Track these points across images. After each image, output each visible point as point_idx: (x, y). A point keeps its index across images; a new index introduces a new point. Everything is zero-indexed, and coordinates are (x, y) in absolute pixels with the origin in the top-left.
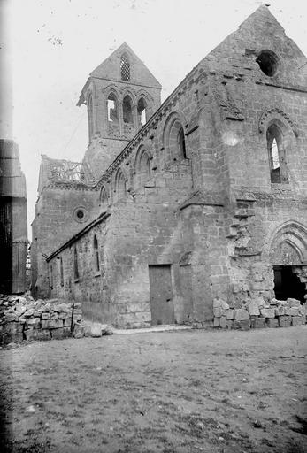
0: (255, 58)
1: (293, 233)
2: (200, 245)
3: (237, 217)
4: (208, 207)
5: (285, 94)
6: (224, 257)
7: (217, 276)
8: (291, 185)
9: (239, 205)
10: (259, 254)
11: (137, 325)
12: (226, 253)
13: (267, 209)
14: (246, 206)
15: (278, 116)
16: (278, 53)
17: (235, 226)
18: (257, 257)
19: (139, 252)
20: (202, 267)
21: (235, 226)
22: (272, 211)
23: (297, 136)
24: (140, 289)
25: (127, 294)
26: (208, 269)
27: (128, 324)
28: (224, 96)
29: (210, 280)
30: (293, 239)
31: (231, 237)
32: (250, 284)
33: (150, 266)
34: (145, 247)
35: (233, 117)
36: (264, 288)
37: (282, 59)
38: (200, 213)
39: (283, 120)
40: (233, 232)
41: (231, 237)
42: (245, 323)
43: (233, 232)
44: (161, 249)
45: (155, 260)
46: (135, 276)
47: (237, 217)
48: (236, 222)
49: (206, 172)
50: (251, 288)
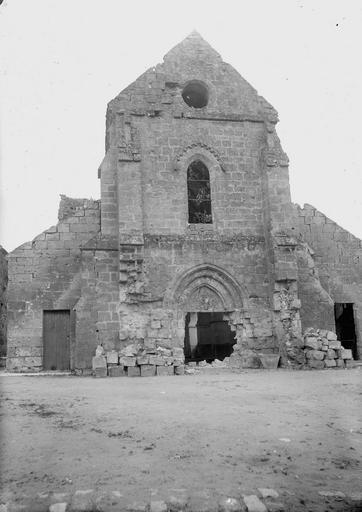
0: (179, 91)
1: (211, 277)
2: (88, 291)
3: (123, 262)
4: (101, 252)
5: (212, 125)
6: (115, 303)
7: (105, 322)
8: (213, 225)
9: (123, 250)
10: (161, 300)
11: (25, 369)
12: (118, 299)
13: (173, 251)
14: (133, 251)
15: (202, 151)
16: (208, 82)
17: (124, 272)
18: (159, 303)
19: (33, 297)
20: (89, 314)
21: (124, 272)
22: (181, 254)
23: (224, 171)
24: (32, 335)
25: (18, 338)
26: (95, 316)
27: (16, 368)
28: (128, 137)
29: (96, 327)
30: (213, 284)
31: (124, 283)
32: (146, 332)
33: (45, 312)
34: (40, 293)
35: (127, 158)
36: (162, 336)
37: (213, 88)
38: (91, 259)
39: (208, 154)
40: (123, 277)
41: (124, 283)
42: (100, 370)
43: (123, 277)
44: (58, 295)
45: (51, 305)
46: (27, 320)
47: (123, 262)
48: (123, 267)
49: (105, 216)
50: (146, 337)
